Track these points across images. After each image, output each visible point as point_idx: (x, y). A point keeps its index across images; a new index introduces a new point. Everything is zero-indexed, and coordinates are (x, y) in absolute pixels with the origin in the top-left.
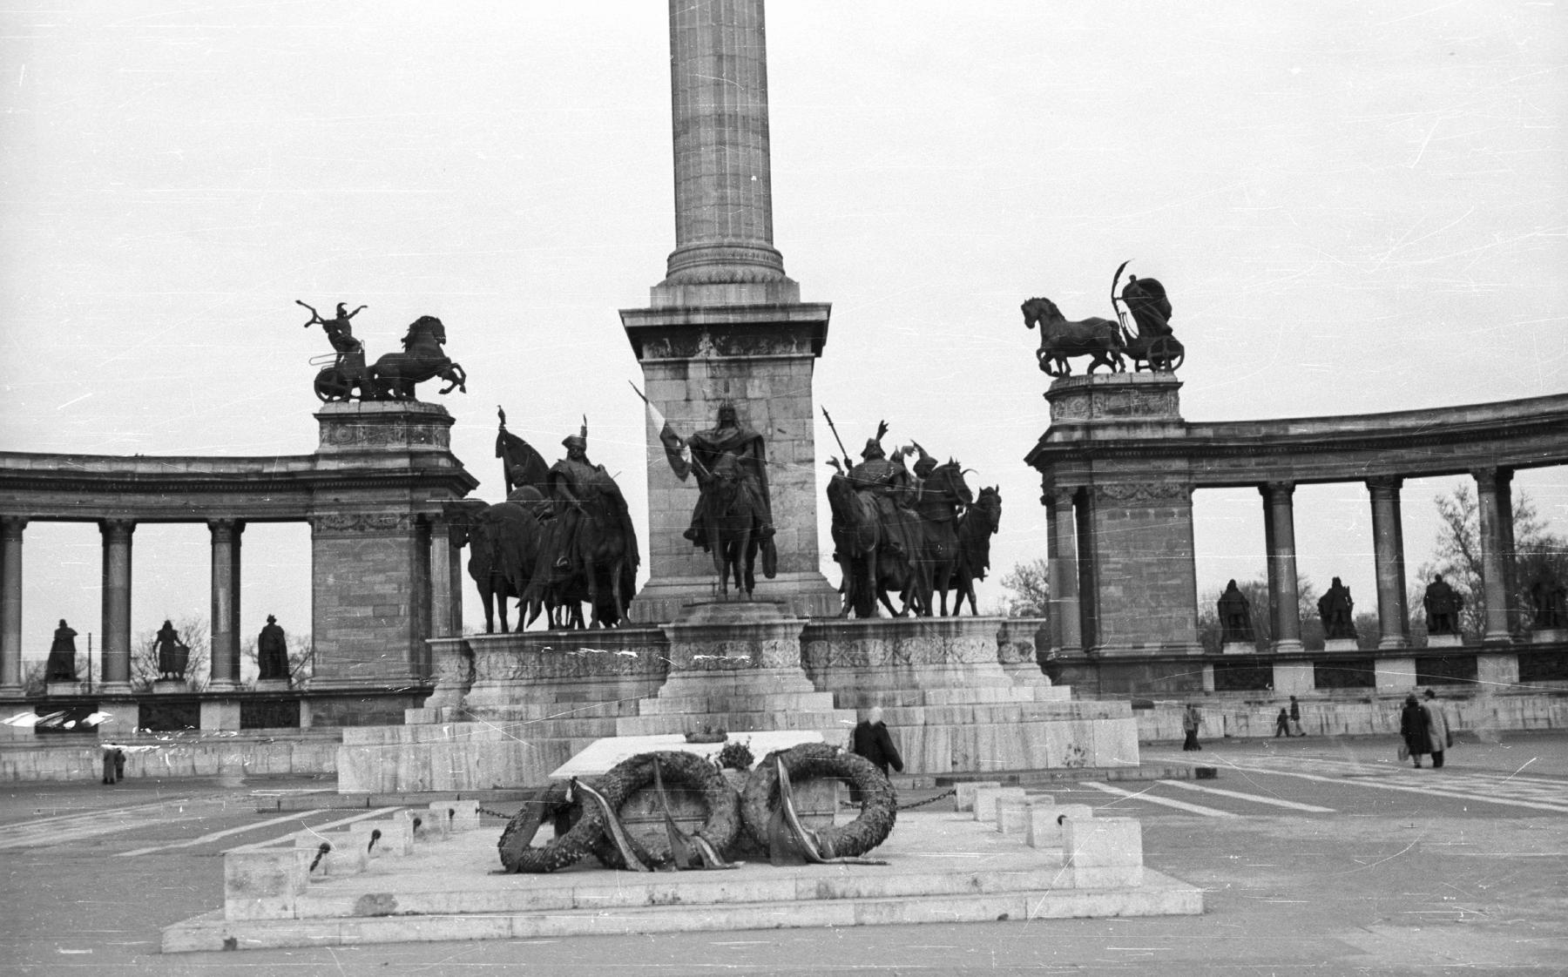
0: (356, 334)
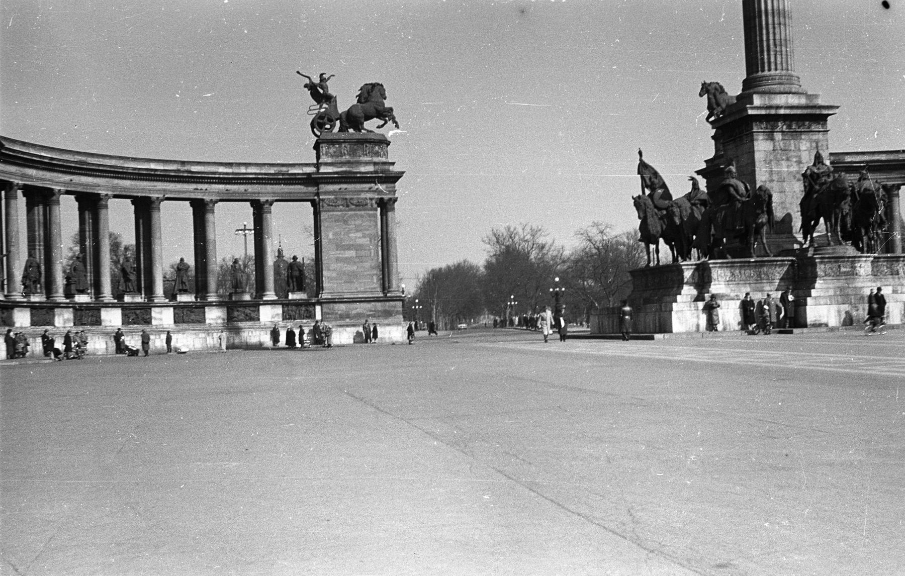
0: (331, 91)
